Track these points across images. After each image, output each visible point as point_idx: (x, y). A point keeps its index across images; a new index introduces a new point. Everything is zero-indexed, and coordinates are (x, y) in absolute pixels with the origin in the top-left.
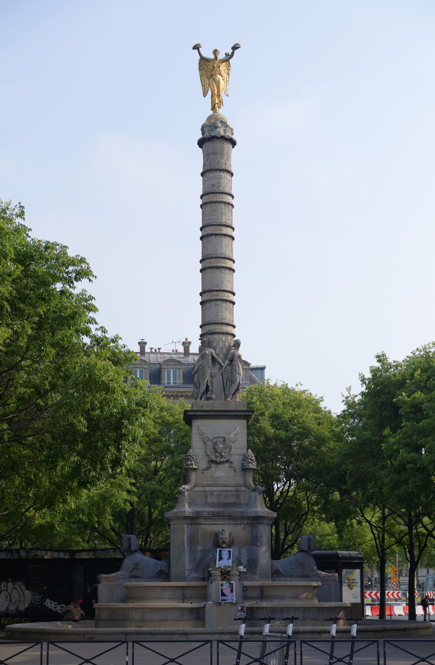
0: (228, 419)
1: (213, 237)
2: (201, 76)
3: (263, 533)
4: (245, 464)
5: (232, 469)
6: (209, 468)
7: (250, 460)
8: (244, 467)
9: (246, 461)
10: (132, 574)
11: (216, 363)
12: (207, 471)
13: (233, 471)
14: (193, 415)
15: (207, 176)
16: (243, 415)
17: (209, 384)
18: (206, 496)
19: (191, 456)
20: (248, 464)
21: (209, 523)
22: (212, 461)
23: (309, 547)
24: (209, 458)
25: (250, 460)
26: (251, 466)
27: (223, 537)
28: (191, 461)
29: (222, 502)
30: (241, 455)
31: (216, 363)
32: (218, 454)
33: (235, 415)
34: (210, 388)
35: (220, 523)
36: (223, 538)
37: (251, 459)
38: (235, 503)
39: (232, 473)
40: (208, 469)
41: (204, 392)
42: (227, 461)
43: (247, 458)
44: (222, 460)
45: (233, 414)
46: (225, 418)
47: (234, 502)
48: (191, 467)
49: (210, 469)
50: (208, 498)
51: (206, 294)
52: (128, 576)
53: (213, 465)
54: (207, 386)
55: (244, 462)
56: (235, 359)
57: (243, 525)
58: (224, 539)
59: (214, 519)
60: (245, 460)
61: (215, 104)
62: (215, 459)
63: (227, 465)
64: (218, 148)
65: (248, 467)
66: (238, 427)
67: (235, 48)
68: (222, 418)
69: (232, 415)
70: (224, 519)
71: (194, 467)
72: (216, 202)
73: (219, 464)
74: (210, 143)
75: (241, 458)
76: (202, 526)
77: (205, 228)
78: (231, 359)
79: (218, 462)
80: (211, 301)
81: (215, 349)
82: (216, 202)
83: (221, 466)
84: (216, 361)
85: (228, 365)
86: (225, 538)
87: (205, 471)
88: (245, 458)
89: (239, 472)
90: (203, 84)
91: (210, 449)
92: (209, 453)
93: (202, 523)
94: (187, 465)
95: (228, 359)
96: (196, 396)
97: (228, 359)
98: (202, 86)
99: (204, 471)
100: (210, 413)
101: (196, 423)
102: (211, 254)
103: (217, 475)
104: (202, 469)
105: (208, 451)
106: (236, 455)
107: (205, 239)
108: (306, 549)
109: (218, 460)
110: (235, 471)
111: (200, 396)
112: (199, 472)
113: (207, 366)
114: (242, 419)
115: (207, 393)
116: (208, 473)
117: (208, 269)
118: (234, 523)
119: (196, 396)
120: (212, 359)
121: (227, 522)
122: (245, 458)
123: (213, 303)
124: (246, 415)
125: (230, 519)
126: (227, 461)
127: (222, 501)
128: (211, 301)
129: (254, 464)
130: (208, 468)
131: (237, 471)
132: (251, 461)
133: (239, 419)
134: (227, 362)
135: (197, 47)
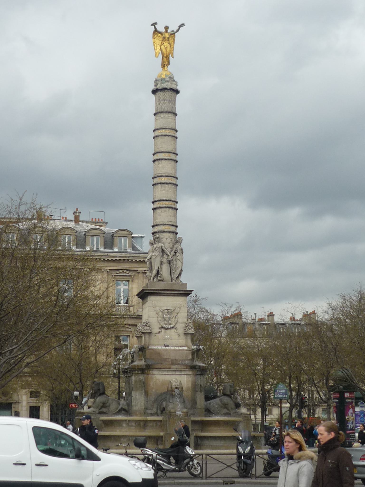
4: (187, 330)
5: (177, 333)
6: (160, 332)
8: (186, 332)
9: (187, 328)
10: (101, 410)
11: (165, 254)
15: (159, 116)
19: (147, 323)
21: (161, 373)
22: (162, 327)
25: (190, 327)
28: (147, 327)
33: (179, 294)
34: (161, 273)
39: (177, 336)
40: (159, 333)
41: (155, 275)
42: (173, 328)
44: (169, 327)
46: (172, 296)
49: (160, 333)
51: (157, 203)
52: (97, 412)
53: (163, 330)
54: (158, 271)
56: (179, 251)
57: (185, 375)
59: (165, 370)
60: (186, 327)
61: (165, 65)
63: (173, 330)
68: (170, 296)
69: (177, 294)
71: (149, 331)
72: (166, 136)
73: (167, 329)
74: (162, 92)
75: (183, 325)
76: (155, 375)
77: (157, 154)
78: (176, 251)
79: (167, 328)
80: (161, 208)
81: (164, 243)
82: (166, 136)
83: (168, 331)
84: (165, 253)
85: (173, 255)
88: (187, 326)
89: (182, 336)
93: (155, 373)
94: (144, 330)
95: (173, 251)
96: (149, 278)
97: (173, 251)
98: (155, 50)
99: (156, 335)
102: (161, 173)
106: (180, 323)
107: (157, 163)
109: (167, 326)
110: (179, 335)
111: (152, 278)
115: (158, 276)
116: (160, 336)
117: (159, 184)
119: (149, 278)
120: (162, 251)
122: (187, 326)
123: (162, 209)
128: (161, 208)
129: (193, 330)
133: (182, 296)
134: (173, 253)
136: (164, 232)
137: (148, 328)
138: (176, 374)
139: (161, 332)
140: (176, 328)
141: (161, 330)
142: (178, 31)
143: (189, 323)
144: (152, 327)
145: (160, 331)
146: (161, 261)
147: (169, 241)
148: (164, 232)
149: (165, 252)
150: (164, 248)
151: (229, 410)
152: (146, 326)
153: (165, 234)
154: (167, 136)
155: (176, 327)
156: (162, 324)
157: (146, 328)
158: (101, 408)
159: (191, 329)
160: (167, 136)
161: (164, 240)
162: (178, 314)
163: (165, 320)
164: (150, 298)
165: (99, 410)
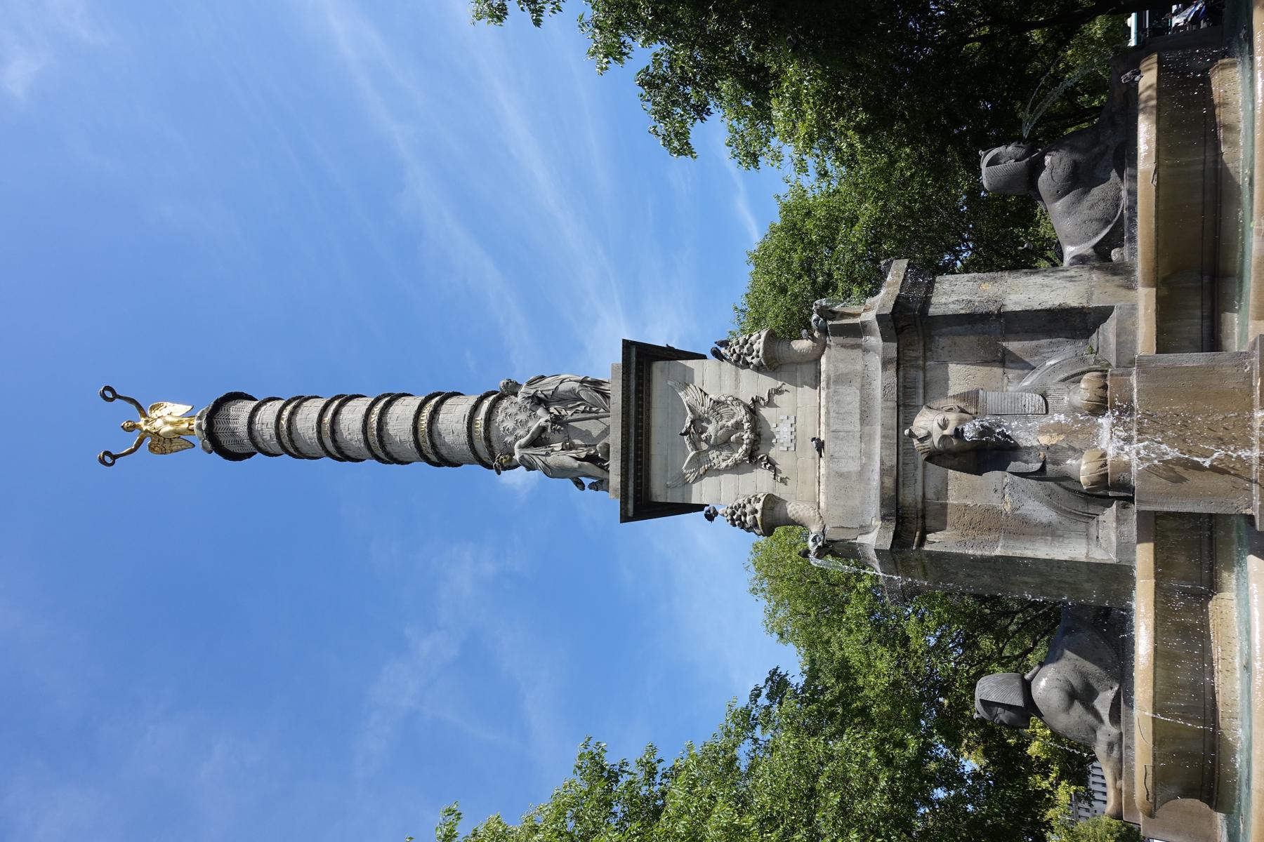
0: (649, 410)
1: (338, 438)
2: (172, 451)
3: (955, 298)
7: (745, 350)
9: (749, 359)
10: (1106, 717)
14: (636, 500)
15: (263, 446)
16: (638, 371)
17: (583, 455)
19: (733, 513)
20: (755, 353)
24: (743, 461)
26: (759, 346)
27: (937, 435)
30: (737, 374)
31: (543, 436)
32: (733, 438)
33: (638, 391)
37: (742, 347)
43: (739, 356)
47: (858, 392)
48: (758, 516)
50: (844, 470)
54: (589, 458)
55: (751, 366)
56: (532, 392)
58: (946, 432)
62: (744, 447)
63: (765, 412)
64: (225, 426)
65: (760, 354)
66: (669, 383)
67: (110, 394)
75: (746, 374)
79: (751, 436)
81: (517, 439)
86: (944, 426)
90: (179, 447)
91: (721, 458)
92: (729, 462)
93: (921, 494)
101: (660, 492)
105: (724, 465)
106: (737, 386)
110: (778, 391)
112: (781, 491)
113: (543, 458)
114: (649, 373)
118: (921, 391)
123: (438, 442)
124: (638, 363)
132: (748, 345)
135: (109, 459)
137: (748, 509)
142: (132, 401)
144: (750, 493)
146: (562, 449)
149: (535, 436)
151: (1103, 154)
152: (743, 518)
155: (750, 402)
156: (740, 453)
158: (1097, 715)
159: (752, 345)
162: (705, 394)
164: (658, 493)
165: (1101, 721)
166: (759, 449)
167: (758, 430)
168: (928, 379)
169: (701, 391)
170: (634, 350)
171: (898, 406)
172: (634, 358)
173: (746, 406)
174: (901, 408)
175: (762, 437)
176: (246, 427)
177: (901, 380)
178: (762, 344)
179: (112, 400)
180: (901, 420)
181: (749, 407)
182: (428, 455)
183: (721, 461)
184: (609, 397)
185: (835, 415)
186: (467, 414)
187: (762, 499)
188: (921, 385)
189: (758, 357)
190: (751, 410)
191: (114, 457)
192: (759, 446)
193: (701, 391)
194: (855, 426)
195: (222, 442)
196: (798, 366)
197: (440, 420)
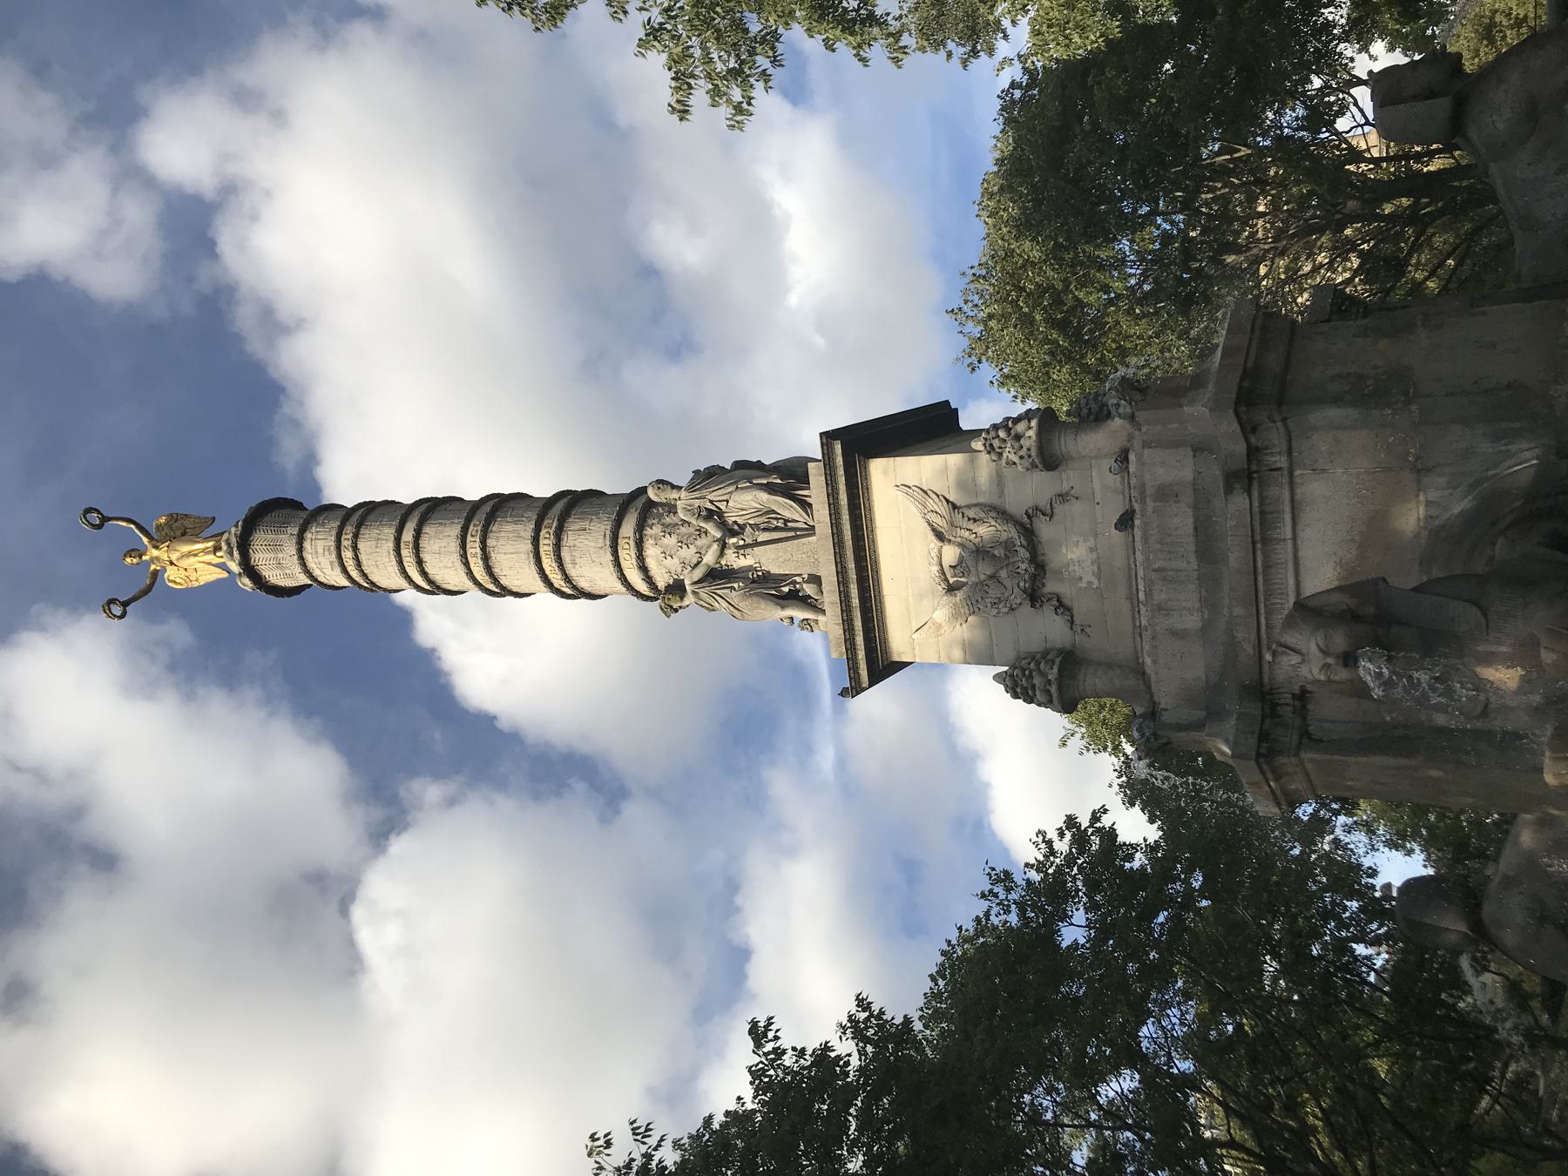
5: (1058, 509)
12: (1075, 613)
13: (1067, 506)
18: (1174, 633)
23: (1432, 94)
29: (1194, 564)
31: (723, 562)
35: (1291, 581)
36: (1326, 666)
38: (1195, 508)
39: (1076, 508)
40: (1069, 609)
44: (1023, 553)
45: (845, 517)
47: (1190, 512)
49: (1067, 602)
53: (1051, 586)
56: (697, 503)
63: (1045, 530)
65: (1033, 453)
70: (1267, 567)
71: (1053, 674)
78: (704, 513)
87: (1077, 620)
89: (1068, 479)
100: (855, 602)
103: (1088, 576)
104: (1067, 630)
106: (1001, 495)
108: (1443, 105)
110: (1063, 497)
114: (866, 477)
116: (1082, 607)
118: (1288, 517)
121: (1284, 552)
125: (1265, 541)
126: (1028, 532)
127: (1189, 563)
130: (1062, 607)
131: (1065, 488)
136: (644, 569)
137: (1037, 681)
138: (1289, 535)
139: (1058, 600)
140: (1029, 517)
141: (1049, 599)
143: (988, 449)
144: (1036, 645)
145: (1055, 602)
147: (670, 541)
148: (644, 569)
150: (699, 573)
152: (1030, 692)
153: (651, 563)
154: (356, 555)
156: (1017, 597)
157: (1038, 693)
160: (356, 555)
161: (673, 564)
163: (992, 577)
166: (1044, 585)
167: (1040, 558)
168: (1297, 497)
169: (948, 501)
170: (838, 447)
171: (1254, 543)
172: (839, 460)
173: (1017, 523)
174: (1259, 546)
175: (1047, 568)
176: (296, 557)
177: (1256, 504)
178: (1034, 437)
179: (99, 527)
180: (1260, 564)
181: (1022, 525)
182: (563, 589)
183: (989, 605)
184: (810, 505)
185: (1158, 546)
186: (608, 533)
187: (1058, 661)
188: (1287, 509)
189: (1030, 456)
190: (1026, 529)
191: (125, 604)
192: (1044, 581)
193: (948, 501)
194: (1188, 562)
195: (267, 577)
196: (1093, 461)
197: (571, 543)
